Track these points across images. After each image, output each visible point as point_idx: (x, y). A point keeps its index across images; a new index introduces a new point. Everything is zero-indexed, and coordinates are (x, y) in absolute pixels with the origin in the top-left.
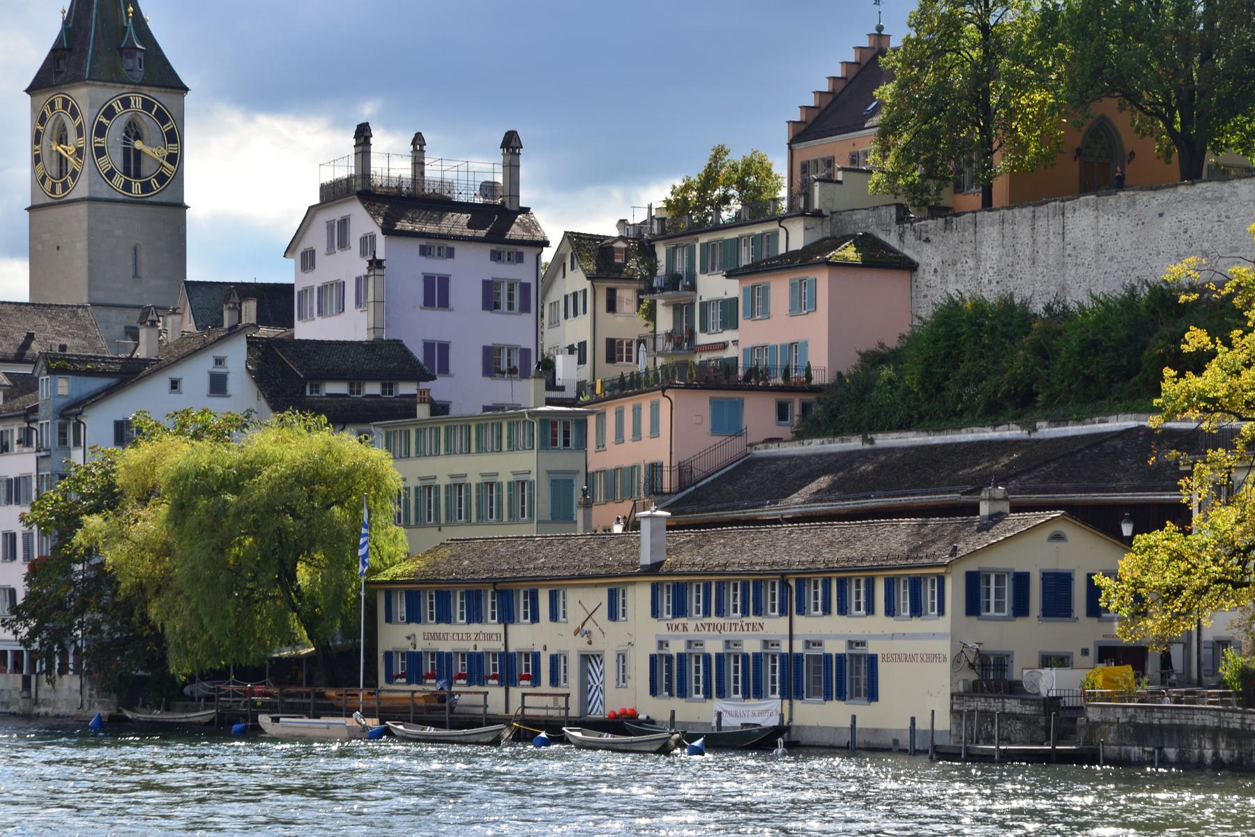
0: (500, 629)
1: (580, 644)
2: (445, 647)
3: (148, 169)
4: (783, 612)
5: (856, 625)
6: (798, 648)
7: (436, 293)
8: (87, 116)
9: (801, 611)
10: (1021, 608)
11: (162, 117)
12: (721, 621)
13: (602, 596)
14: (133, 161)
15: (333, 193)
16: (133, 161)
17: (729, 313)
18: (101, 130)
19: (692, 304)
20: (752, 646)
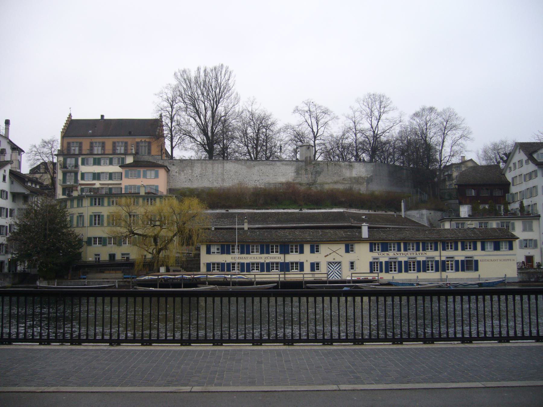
0: (282, 256)
1: (330, 259)
2: (245, 261)
4: (436, 249)
5: (469, 253)
6: (443, 259)
9: (444, 249)
12: (407, 252)
13: (343, 247)
19: (76, 174)
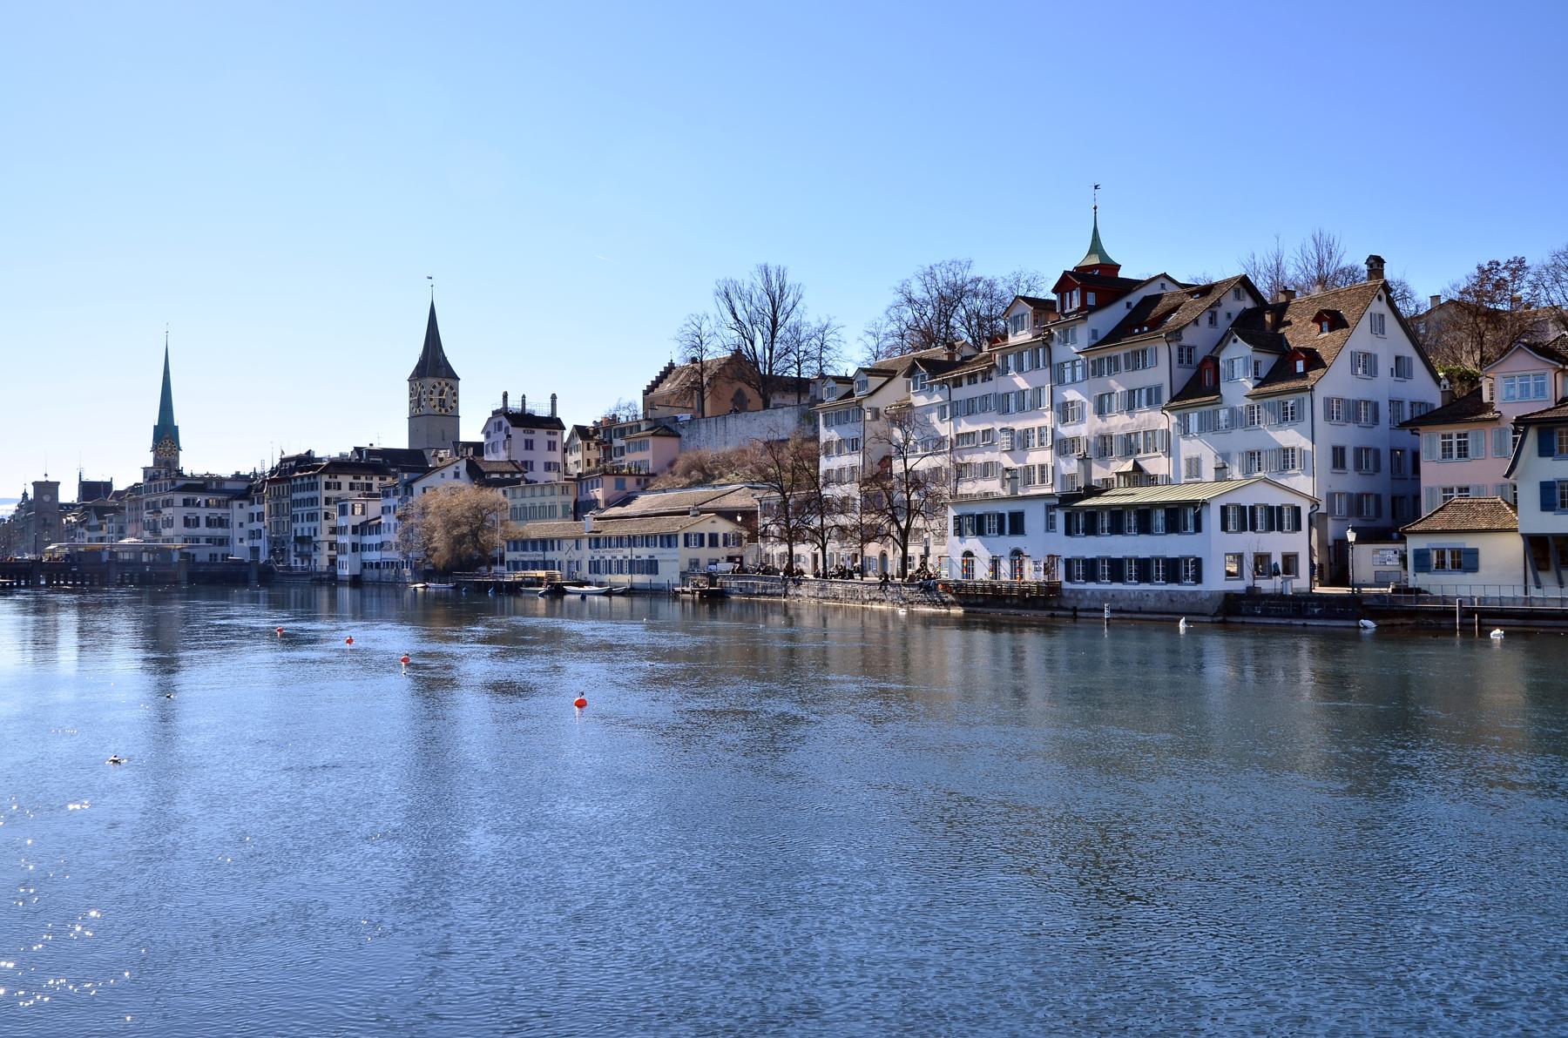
3: (448, 404)
7: (529, 445)
8: (428, 388)
10: (702, 544)
14: (442, 403)
15: (495, 413)
16: (442, 403)
17: (622, 451)
20: (620, 557)
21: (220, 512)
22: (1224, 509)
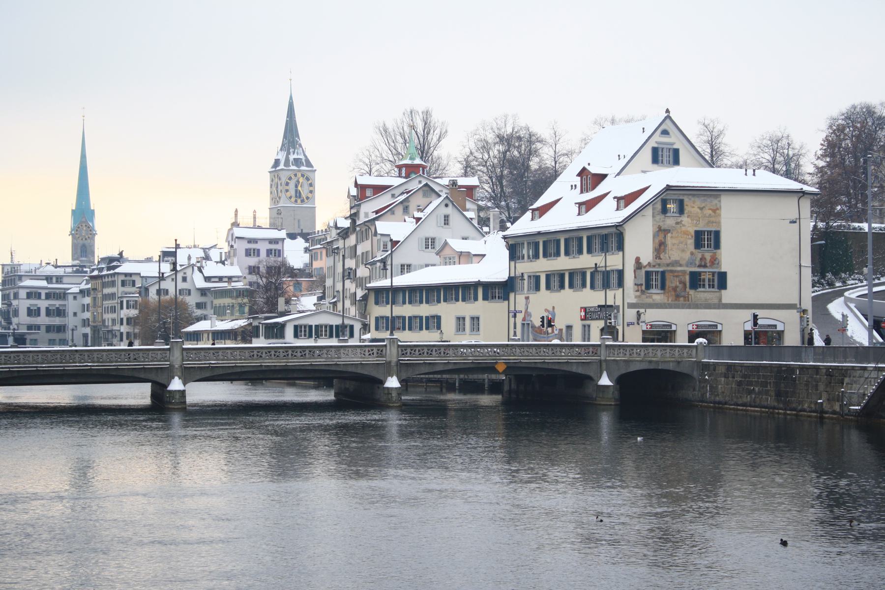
11: (308, 179)
14: (298, 194)
18: (287, 184)
21: (57, 303)
22: (296, 327)
